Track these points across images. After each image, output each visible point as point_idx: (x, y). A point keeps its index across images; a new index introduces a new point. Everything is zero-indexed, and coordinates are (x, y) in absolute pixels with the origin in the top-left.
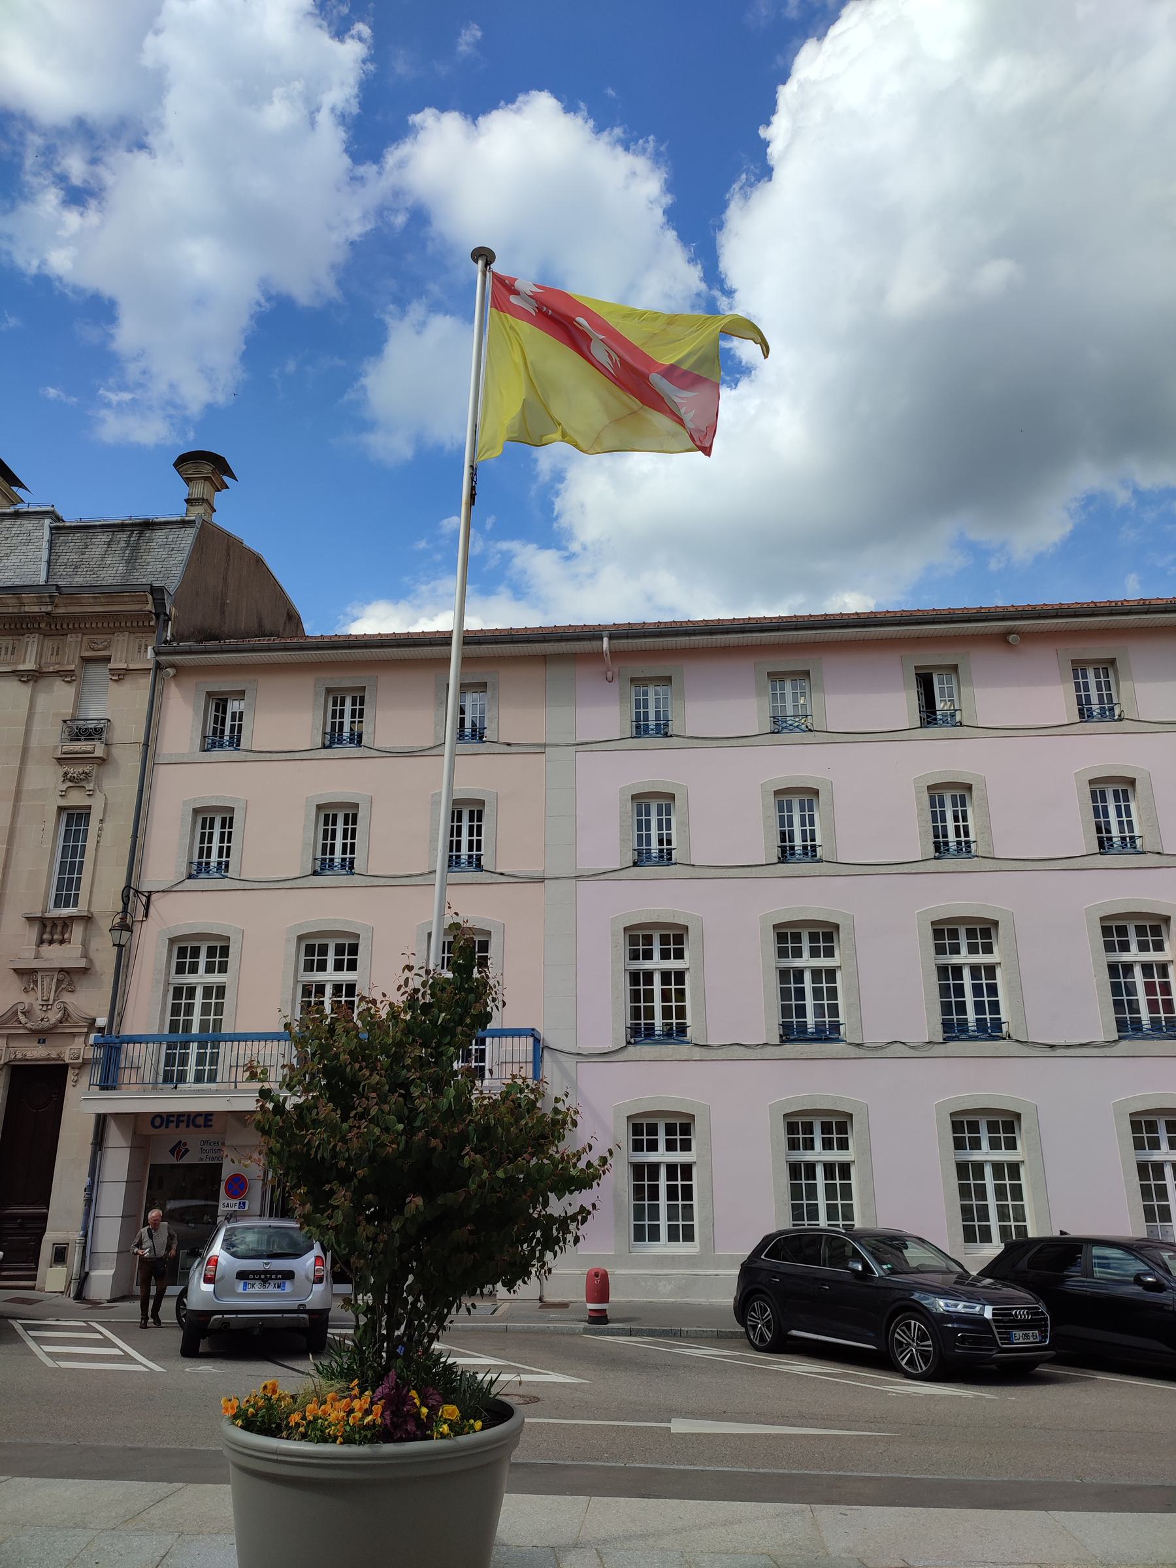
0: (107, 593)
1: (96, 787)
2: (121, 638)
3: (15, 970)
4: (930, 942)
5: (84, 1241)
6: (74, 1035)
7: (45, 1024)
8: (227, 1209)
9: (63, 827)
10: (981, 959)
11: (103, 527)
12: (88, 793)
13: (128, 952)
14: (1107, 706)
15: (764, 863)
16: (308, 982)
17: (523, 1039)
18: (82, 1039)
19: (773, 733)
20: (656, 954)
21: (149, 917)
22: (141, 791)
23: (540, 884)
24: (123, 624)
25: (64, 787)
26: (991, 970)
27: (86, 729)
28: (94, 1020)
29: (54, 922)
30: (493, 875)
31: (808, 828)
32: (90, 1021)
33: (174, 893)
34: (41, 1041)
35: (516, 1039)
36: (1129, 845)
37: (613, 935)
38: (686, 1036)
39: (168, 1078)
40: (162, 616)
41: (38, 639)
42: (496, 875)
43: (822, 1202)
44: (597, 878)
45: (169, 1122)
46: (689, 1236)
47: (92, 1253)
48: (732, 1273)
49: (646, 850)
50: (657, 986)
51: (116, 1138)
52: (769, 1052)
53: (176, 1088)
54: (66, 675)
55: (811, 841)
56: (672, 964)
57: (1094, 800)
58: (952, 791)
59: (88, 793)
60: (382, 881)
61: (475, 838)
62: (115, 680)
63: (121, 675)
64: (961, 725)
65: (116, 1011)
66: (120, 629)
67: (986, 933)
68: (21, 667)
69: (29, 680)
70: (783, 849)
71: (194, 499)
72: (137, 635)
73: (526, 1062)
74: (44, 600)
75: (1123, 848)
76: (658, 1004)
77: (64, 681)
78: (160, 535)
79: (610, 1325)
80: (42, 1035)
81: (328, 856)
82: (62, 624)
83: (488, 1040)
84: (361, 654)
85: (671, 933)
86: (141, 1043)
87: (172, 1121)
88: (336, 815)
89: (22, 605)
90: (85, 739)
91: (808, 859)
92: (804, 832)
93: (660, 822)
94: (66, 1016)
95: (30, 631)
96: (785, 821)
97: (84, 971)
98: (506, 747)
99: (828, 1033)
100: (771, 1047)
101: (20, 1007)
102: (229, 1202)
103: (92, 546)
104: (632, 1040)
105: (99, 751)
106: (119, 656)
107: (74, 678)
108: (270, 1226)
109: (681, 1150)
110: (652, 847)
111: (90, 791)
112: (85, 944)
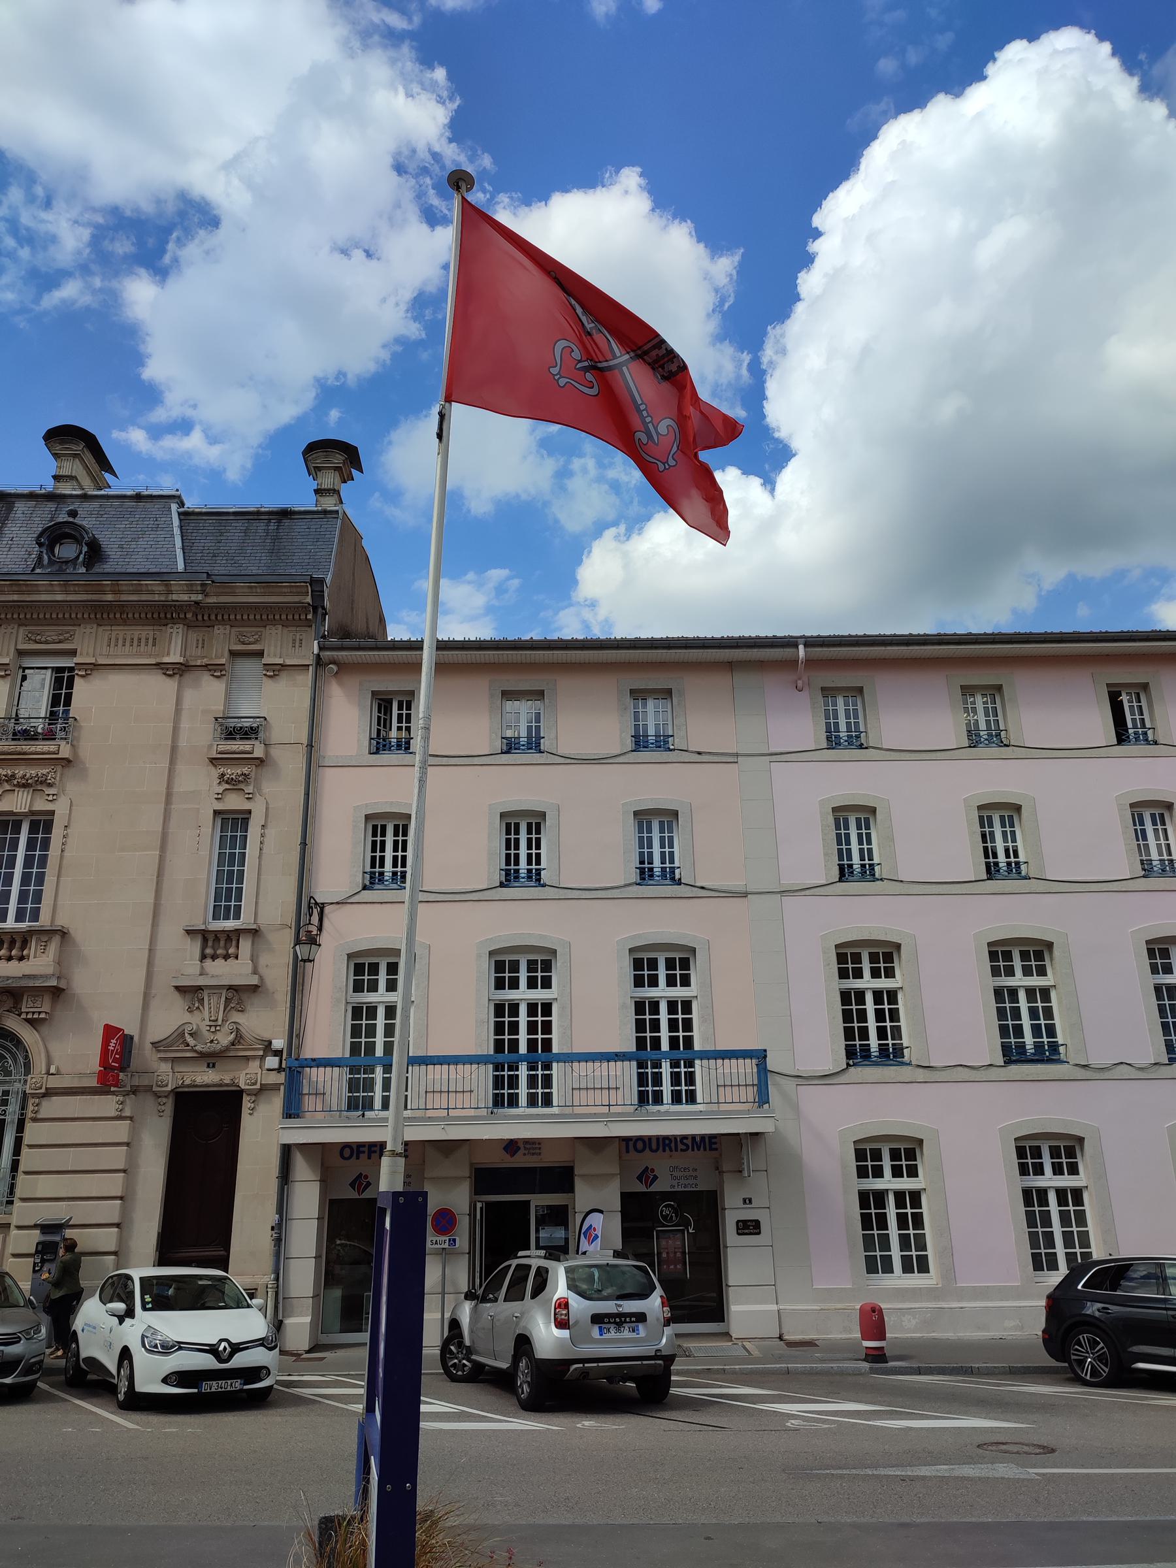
0: (266, 584)
1: (256, 790)
2: (274, 631)
3: (177, 988)
4: (987, 965)
5: (276, 1285)
6: (247, 1058)
7: (216, 1047)
8: (436, 1246)
9: (219, 834)
10: (1035, 981)
11: (235, 514)
12: (247, 796)
13: (302, 968)
14: (1140, 730)
15: (974, 879)
16: (500, 1000)
17: (626, 1063)
18: (257, 1063)
19: (970, 747)
20: (867, 973)
21: (324, 933)
22: (307, 794)
23: (744, 899)
24: (277, 617)
25: (220, 789)
26: (1045, 993)
27: (241, 728)
28: (270, 1043)
29: (217, 935)
30: (693, 888)
31: (865, 846)
32: (266, 1043)
33: (349, 906)
34: (211, 1065)
35: (734, 1061)
36: (1014, 870)
37: (824, 953)
38: (903, 1058)
39: (353, 1105)
40: (320, 610)
41: (183, 631)
42: (696, 889)
43: (1057, 1229)
44: (803, 893)
45: (359, 1152)
46: (924, 1267)
47: (284, 1298)
48: (978, 1305)
49: (670, 868)
50: (870, 1006)
51: (302, 1169)
52: (994, 1073)
53: (363, 1114)
54: (216, 670)
55: (649, 863)
56: (883, 983)
57: (982, 825)
58: (999, 811)
59: (247, 796)
60: (576, 894)
61: (534, 851)
62: (270, 677)
63: (275, 671)
64: (1156, 743)
65: (295, 1034)
66: (274, 622)
67: (1039, 956)
68: (166, 660)
69: (174, 674)
70: (841, 868)
71: (324, 490)
72: (290, 629)
73: (739, 1085)
74: (194, 588)
75: (1009, 873)
76: (872, 1024)
77: (213, 675)
78: (300, 526)
79: (891, 1364)
80: (211, 1059)
81: (512, 867)
82: (209, 615)
83: (555, 1065)
84: (482, 656)
85: (881, 951)
86: (339, 1067)
87: (364, 1152)
88: (386, 825)
89: (170, 592)
90: (241, 739)
91: (668, 882)
92: (663, 854)
93: (860, 836)
94: (239, 1038)
95: (174, 621)
96: (644, 843)
97: (254, 989)
98: (697, 755)
99: (1047, 1053)
100: (995, 1068)
101: (188, 1028)
102: (438, 1239)
103: (228, 534)
104: (851, 1062)
105: (259, 752)
106: (272, 648)
107: (223, 673)
108: (608, 1264)
109: (907, 1177)
110: (853, 862)
111: (249, 794)
112: (254, 959)
